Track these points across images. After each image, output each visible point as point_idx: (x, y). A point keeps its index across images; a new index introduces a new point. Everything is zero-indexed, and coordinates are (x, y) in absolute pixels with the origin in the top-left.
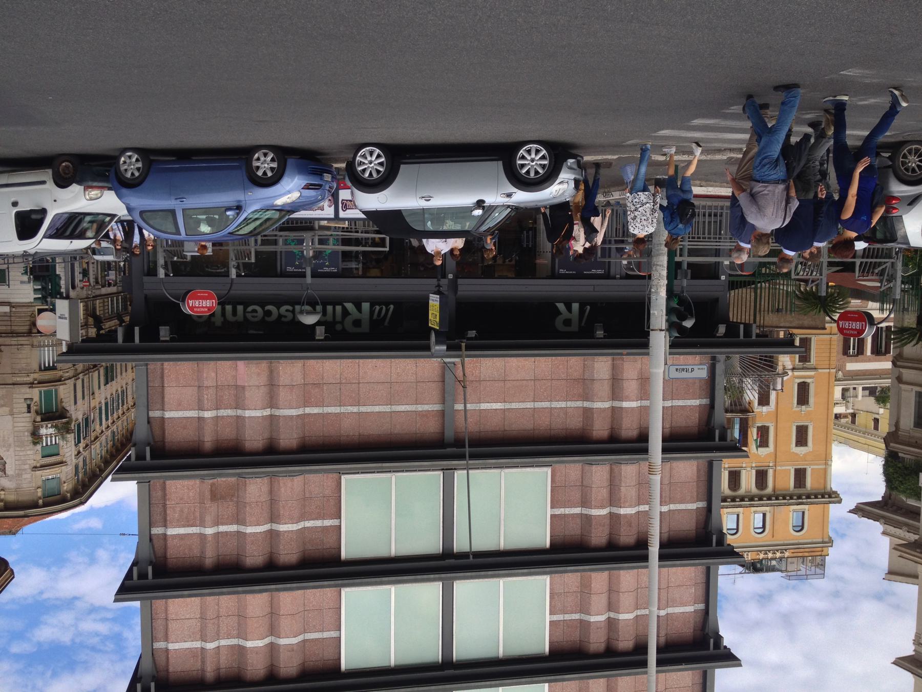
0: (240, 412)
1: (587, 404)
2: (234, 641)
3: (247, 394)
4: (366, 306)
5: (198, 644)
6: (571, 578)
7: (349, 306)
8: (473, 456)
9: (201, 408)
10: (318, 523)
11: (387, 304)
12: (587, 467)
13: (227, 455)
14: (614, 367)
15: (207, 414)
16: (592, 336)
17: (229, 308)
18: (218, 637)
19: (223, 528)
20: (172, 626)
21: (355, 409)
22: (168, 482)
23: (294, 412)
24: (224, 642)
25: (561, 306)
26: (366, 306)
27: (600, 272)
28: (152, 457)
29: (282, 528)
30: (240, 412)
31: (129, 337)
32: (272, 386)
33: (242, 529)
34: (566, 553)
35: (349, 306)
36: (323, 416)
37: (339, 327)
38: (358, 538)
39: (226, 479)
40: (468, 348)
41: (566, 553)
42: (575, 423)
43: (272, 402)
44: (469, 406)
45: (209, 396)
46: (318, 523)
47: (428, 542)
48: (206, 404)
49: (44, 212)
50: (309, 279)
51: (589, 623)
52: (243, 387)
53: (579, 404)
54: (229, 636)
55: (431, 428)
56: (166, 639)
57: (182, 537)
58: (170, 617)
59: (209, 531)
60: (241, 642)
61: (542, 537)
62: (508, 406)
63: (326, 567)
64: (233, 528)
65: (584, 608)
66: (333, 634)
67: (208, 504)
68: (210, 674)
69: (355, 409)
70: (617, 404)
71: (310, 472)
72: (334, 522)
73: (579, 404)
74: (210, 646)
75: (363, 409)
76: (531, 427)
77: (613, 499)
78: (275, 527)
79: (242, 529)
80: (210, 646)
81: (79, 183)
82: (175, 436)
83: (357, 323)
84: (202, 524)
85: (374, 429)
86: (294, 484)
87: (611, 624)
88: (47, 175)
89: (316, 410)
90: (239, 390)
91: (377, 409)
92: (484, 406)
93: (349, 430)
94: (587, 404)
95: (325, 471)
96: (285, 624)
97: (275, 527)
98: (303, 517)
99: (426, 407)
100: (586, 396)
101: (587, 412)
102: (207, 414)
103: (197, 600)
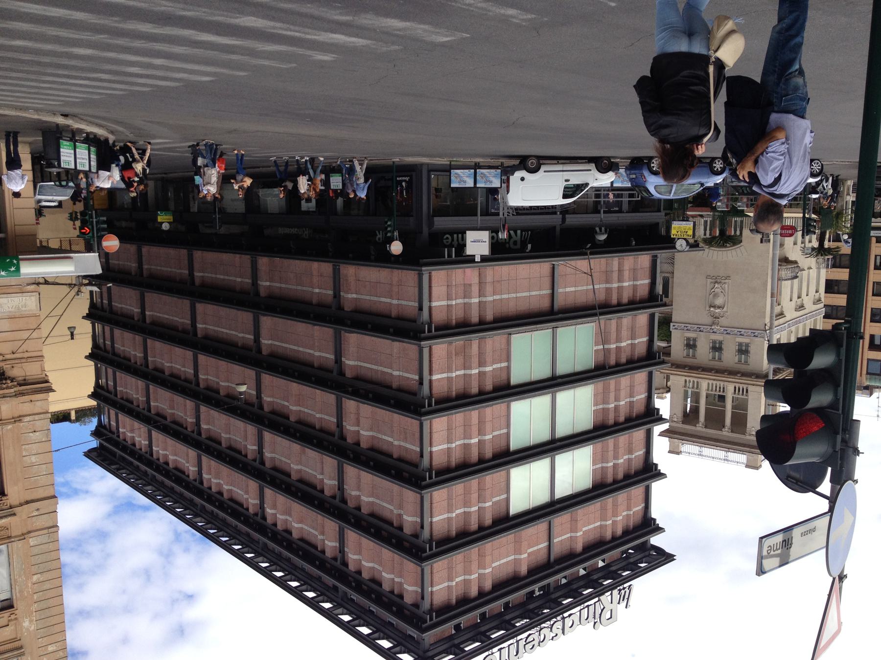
0: (466, 300)
1: (608, 286)
2: (461, 442)
3: (473, 288)
4: (519, 232)
6: (600, 383)
7: (512, 232)
8: (602, 314)
9: (449, 298)
10: (498, 365)
11: (527, 230)
12: (608, 322)
13: (462, 328)
14: (619, 264)
15: (454, 303)
16: (629, 244)
17: (460, 235)
19: (458, 373)
20: (435, 436)
21: (514, 295)
22: (434, 347)
23: (490, 299)
25: (597, 229)
26: (519, 232)
27: (617, 209)
28: (435, 331)
29: (488, 369)
30: (466, 300)
31: (450, 256)
32: (481, 283)
33: (468, 372)
34: (598, 372)
35: (512, 232)
36: (501, 300)
37: (507, 245)
38: (521, 371)
39: (458, 341)
40: (592, 254)
41: (598, 372)
42: (601, 297)
43: (481, 294)
44: (591, 287)
46: (498, 365)
47: (542, 371)
48: (454, 297)
49: (587, 184)
50: (602, 215)
51: (608, 409)
52: (470, 285)
53: (604, 286)
55: (545, 304)
56: (431, 446)
57: (439, 380)
58: (434, 430)
59: (454, 375)
60: (466, 441)
61: (590, 364)
62: (577, 289)
63: (507, 391)
64: (461, 372)
65: (605, 401)
66: (505, 431)
67: (454, 357)
68: (453, 464)
69: (514, 295)
70: (620, 284)
71: (495, 335)
72: (504, 364)
73: (604, 286)
75: (519, 295)
76: (585, 300)
77: (619, 339)
78: (482, 369)
79: (468, 372)
80: (454, 445)
81: (613, 171)
82: (439, 317)
83: (515, 243)
84: (450, 370)
85: (523, 307)
86: (494, 340)
87: (616, 408)
88: (592, 166)
89: (497, 297)
90: (467, 287)
91: (524, 294)
92: (568, 290)
93: (512, 308)
94: (608, 286)
95: (499, 334)
96: (488, 426)
97: (482, 369)
98: (494, 363)
99: (545, 292)
100: (607, 282)
101: (608, 291)
102: (454, 303)
103: (445, 418)
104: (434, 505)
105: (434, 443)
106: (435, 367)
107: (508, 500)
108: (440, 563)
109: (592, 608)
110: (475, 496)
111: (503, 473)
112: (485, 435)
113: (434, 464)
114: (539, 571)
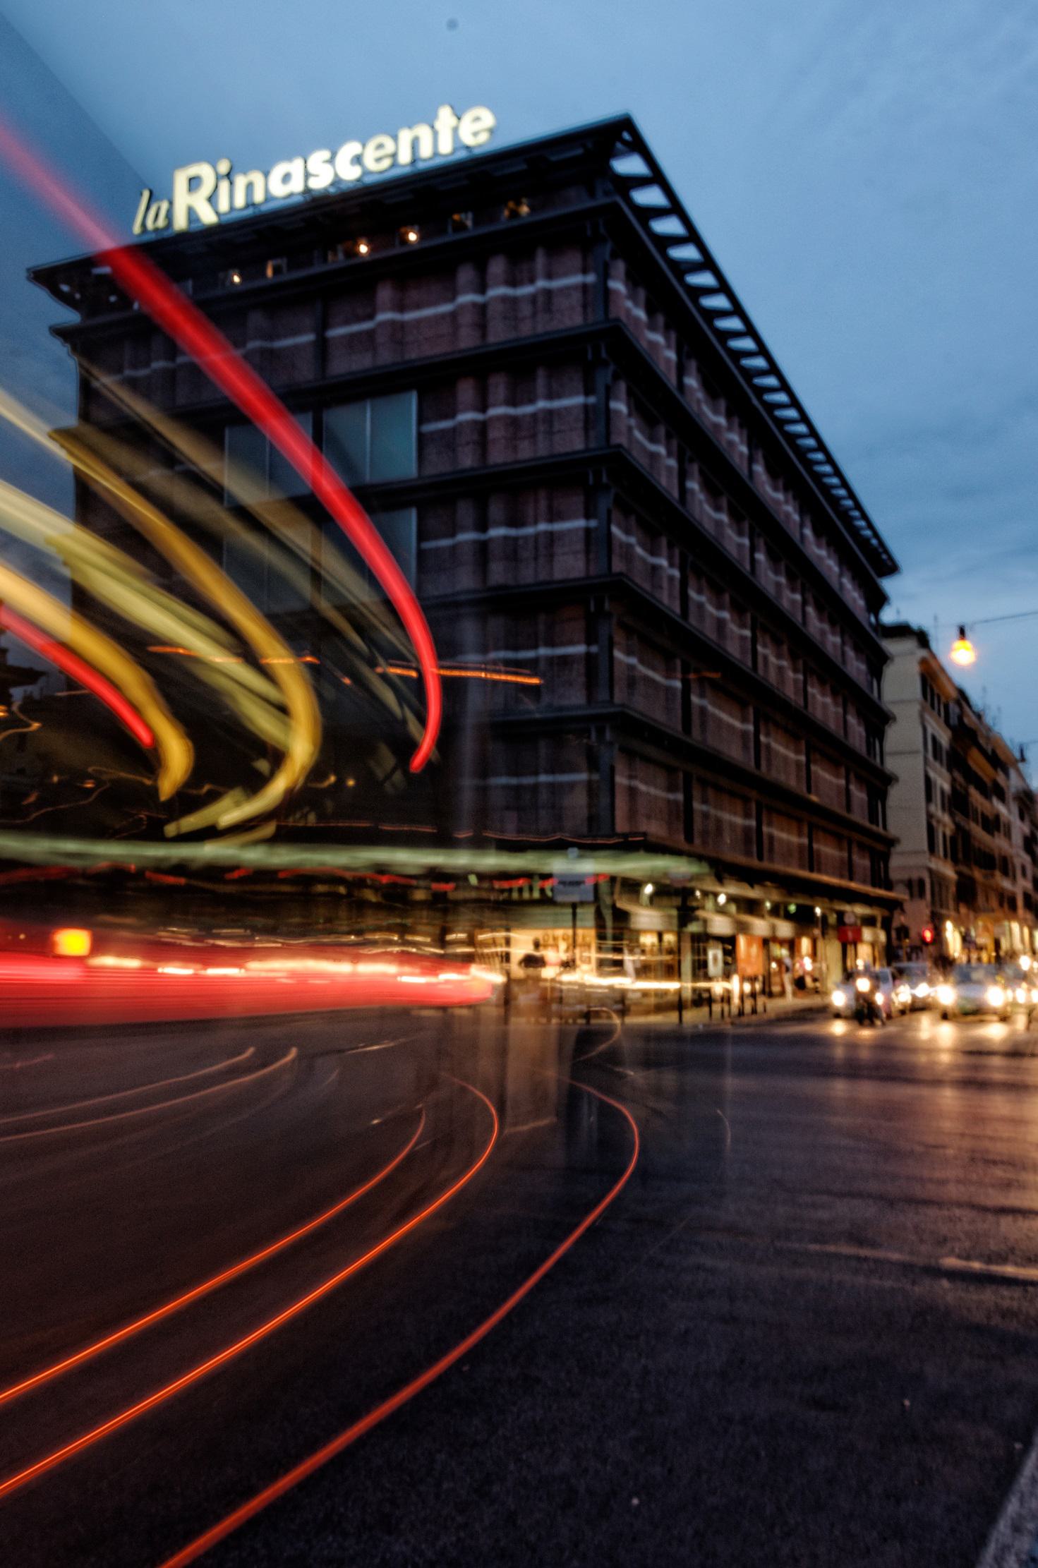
0: (514, 781)
5: (558, 526)
9: (552, 787)
18: (537, 537)
20: (580, 546)
24: (530, 530)
30: (514, 781)
45: (544, 796)
52: (507, 808)
54: (526, 538)
58: (581, 556)
60: (512, 532)
66: (427, 545)
74: (543, 527)
102: (543, 778)
103: (558, 575)
104: (581, 425)
105: (581, 534)
106: (580, 668)
107: (421, 420)
108: (568, 323)
109: (240, 202)
110: (495, 433)
111: (430, 470)
112: (475, 542)
113: (582, 498)
114: (357, 285)
